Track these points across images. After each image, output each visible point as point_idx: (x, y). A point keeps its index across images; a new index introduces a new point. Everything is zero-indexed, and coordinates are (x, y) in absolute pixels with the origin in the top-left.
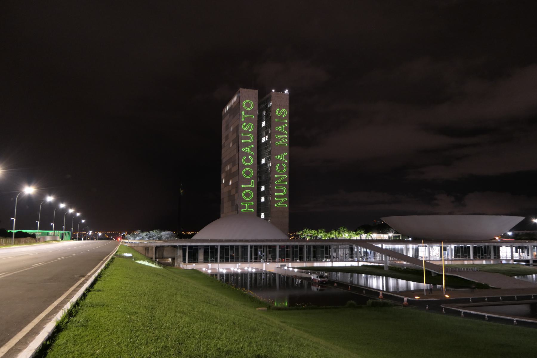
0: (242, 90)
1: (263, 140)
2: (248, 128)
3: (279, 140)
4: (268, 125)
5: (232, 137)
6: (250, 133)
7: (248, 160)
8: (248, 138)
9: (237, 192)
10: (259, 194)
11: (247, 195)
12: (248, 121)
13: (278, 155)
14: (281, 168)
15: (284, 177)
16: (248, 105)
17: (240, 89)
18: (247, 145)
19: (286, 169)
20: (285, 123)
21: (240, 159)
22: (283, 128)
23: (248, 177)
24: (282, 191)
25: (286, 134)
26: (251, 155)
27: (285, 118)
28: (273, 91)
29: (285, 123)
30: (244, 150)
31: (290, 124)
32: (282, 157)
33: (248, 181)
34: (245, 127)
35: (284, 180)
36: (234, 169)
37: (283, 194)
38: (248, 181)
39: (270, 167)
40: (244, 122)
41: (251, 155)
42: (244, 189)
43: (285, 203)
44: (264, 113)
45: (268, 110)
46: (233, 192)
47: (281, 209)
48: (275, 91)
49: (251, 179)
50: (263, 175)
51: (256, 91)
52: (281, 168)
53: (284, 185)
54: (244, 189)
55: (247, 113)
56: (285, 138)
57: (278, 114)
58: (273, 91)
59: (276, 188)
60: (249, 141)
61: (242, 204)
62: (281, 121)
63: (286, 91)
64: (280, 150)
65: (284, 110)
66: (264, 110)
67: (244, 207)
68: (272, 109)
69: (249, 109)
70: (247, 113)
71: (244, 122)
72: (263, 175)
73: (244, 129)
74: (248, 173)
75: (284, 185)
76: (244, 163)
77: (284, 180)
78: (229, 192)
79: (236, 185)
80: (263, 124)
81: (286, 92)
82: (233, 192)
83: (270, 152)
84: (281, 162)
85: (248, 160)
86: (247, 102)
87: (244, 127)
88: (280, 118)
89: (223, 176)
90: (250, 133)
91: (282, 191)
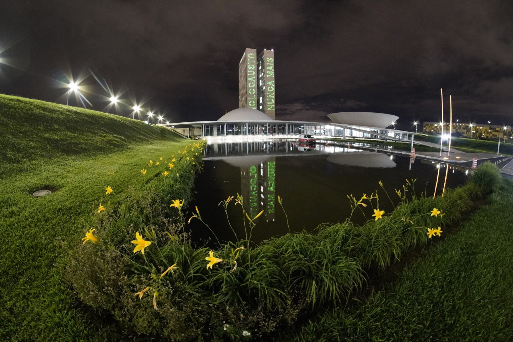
0: (248, 50)
1: (260, 76)
5: (243, 75)
7: (252, 85)
9: (246, 103)
10: (259, 104)
11: (252, 104)
18: (251, 77)
19: (273, 90)
20: (271, 65)
24: (271, 101)
33: (252, 96)
36: (245, 91)
38: (252, 96)
42: (250, 100)
43: (273, 108)
44: (260, 62)
45: (262, 60)
46: (244, 103)
50: (260, 92)
51: (255, 50)
52: (271, 89)
53: (273, 98)
54: (250, 100)
55: (251, 60)
57: (268, 61)
63: (272, 50)
64: (270, 79)
70: (251, 60)
72: (260, 92)
75: (273, 98)
76: (250, 86)
78: (243, 104)
79: (246, 100)
80: (260, 68)
82: (244, 103)
84: (270, 86)
87: (249, 67)
88: (269, 62)
89: (240, 97)
91: (271, 101)
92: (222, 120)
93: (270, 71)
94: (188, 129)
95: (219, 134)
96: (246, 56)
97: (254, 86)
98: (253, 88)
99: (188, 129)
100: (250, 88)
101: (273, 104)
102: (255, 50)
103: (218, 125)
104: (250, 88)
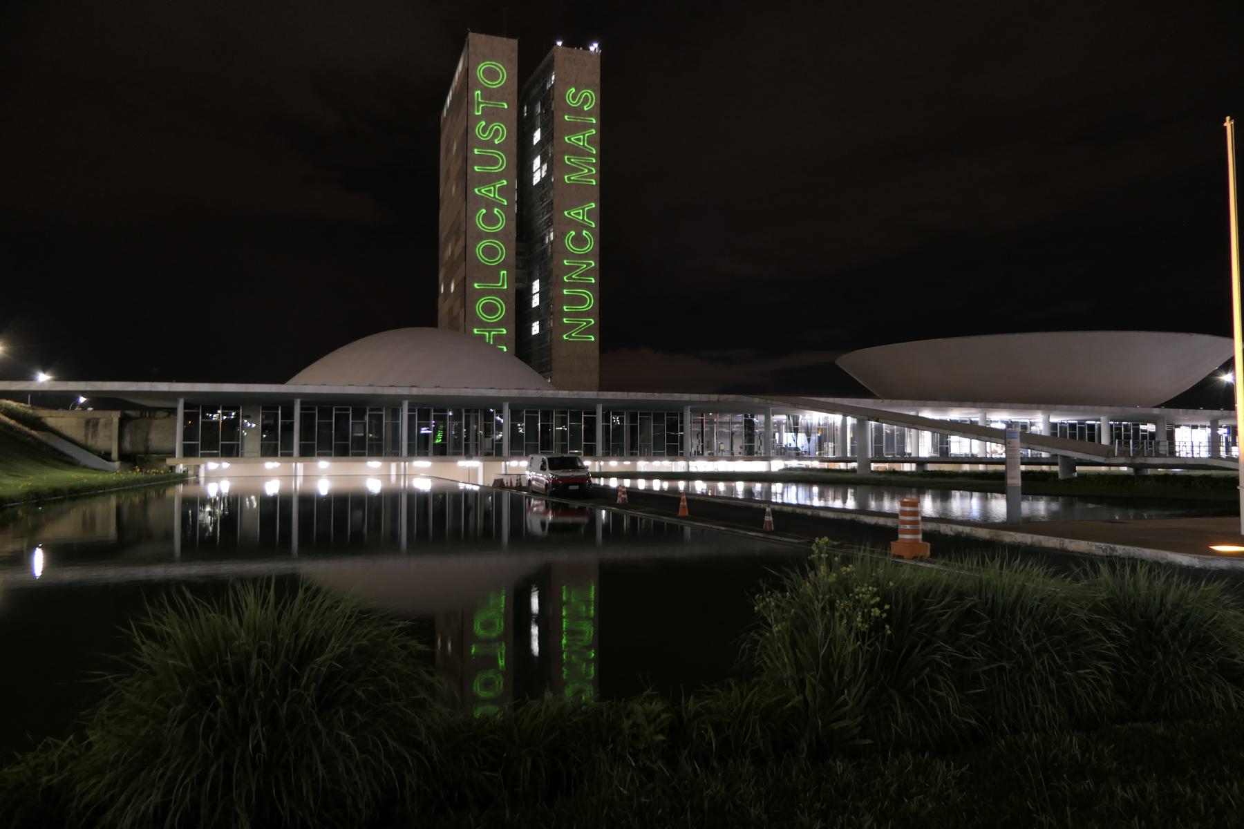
0: (476, 40)
2: (491, 134)
3: (574, 170)
4: (547, 138)
6: (498, 147)
7: (490, 219)
8: (493, 161)
9: (464, 306)
11: (490, 309)
12: (490, 115)
13: (570, 207)
14: (579, 241)
15: (589, 264)
17: (471, 35)
18: (487, 179)
19: (590, 246)
20: (588, 126)
21: (468, 218)
22: (584, 139)
23: (493, 262)
24: (582, 301)
25: (591, 155)
26: (500, 206)
27: (589, 113)
29: (590, 126)
31: (604, 127)
32: (583, 214)
34: (484, 130)
39: (551, 243)
40: (479, 118)
41: (500, 206)
43: (588, 331)
51: (514, 43)
52: (579, 241)
53: (588, 286)
55: (488, 94)
56: (592, 165)
57: (572, 103)
58: (560, 44)
59: (565, 292)
60: (495, 169)
62: (580, 119)
64: (578, 194)
65: (587, 92)
66: (532, 98)
68: (556, 92)
69: (495, 85)
70: (488, 94)
75: (588, 286)
76: (481, 225)
79: (463, 286)
83: (552, 203)
84: (579, 226)
85: (490, 219)
86: (489, 70)
88: (578, 111)
90: (498, 147)
92: (315, 381)
93: (576, 151)
94: (115, 416)
95: (269, 451)
96: (467, 71)
97: (500, 226)
98: (495, 236)
99: (115, 416)
100: (483, 236)
101: (587, 314)
103: (269, 405)
104: (483, 236)
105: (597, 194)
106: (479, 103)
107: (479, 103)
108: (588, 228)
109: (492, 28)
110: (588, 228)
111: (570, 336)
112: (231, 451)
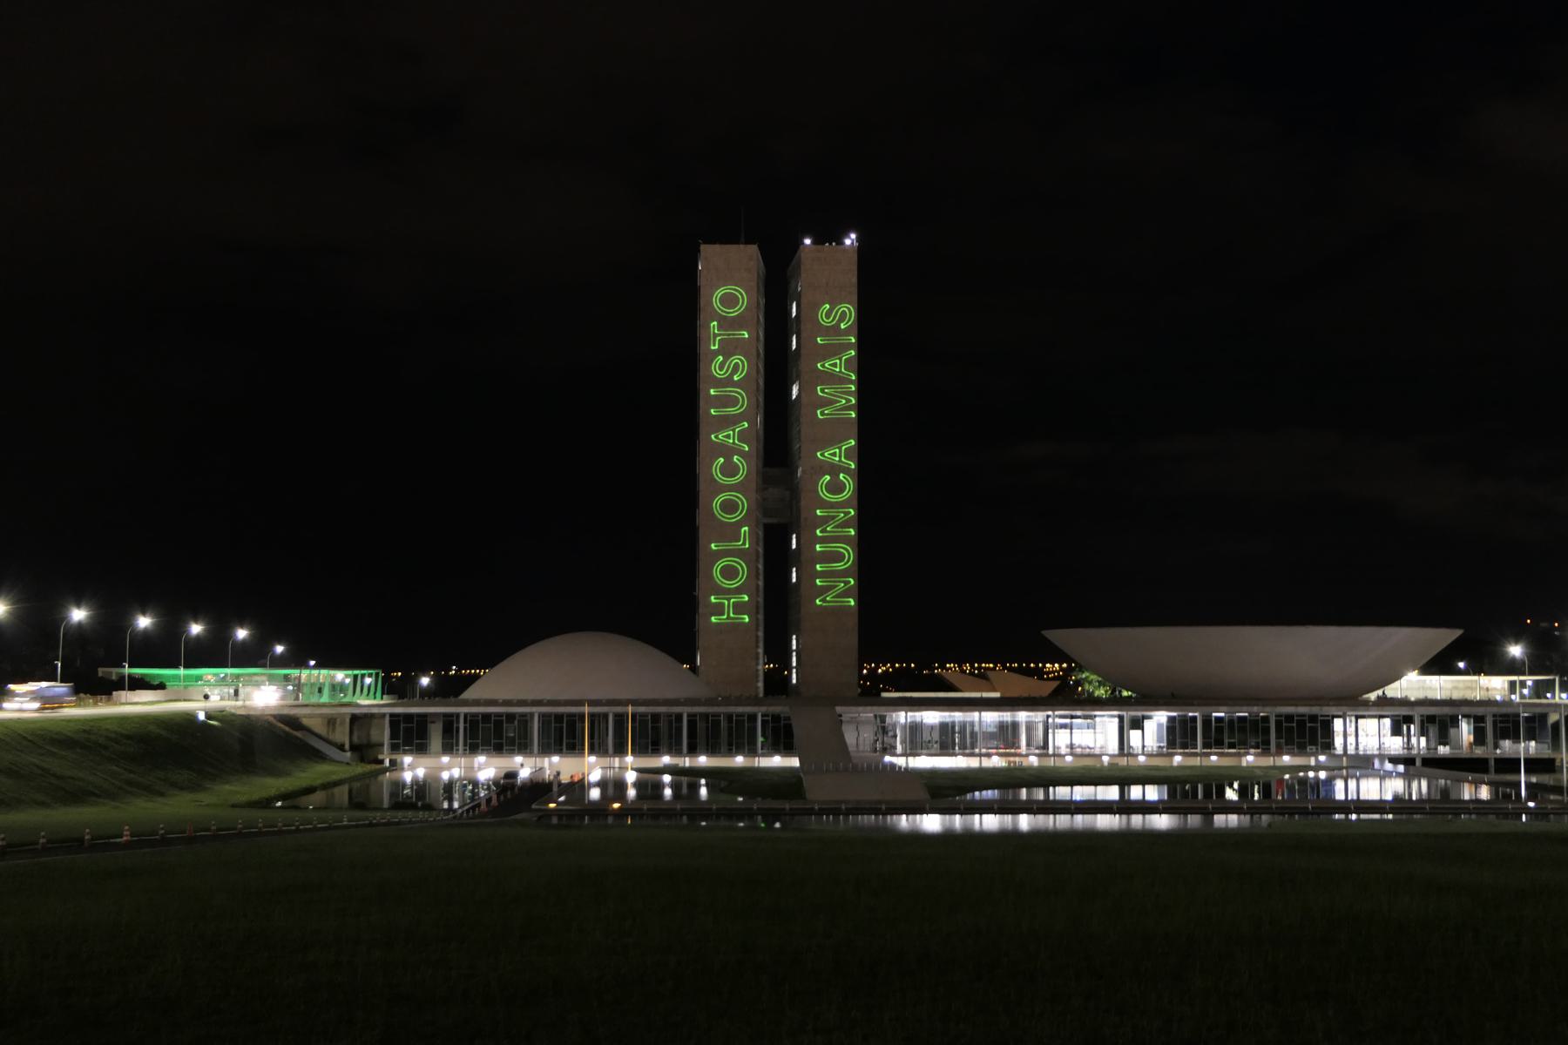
7: (729, 470)
8: (732, 402)
11: (729, 573)
12: (728, 349)
14: (836, 487)
16: (729, 301)
18: (727, 422)
24: (838, 557)
28: (808, 241)
30: (719, 437)
31: (861, 347)
33: (732, 532)
35: (845, 524)
37: (840, 566)
40: (716, 353)
43: (845, 594)
47: (838, 612)
48: (814, 243)
49: (739, 525)
51: (753, 250)
52: (836, 487)
53: (845, 540)
55: (726, 324)
58: (808, 241)
61: (713, 599)
67: (719, 609)
69: (733, 313)
70: (726, 324)
71: (716, 353)
73: (719, 374)
74: (729, 507)
77: (845, 524)
81: (848, 242)
91: (838, 557)
93: (831, 378)
102: (747, 256)
105: (855, 430)
106: (715, 336)
107: (715, 336)
108: (847, 471)
109: (727, 237)
110: (847, 471)
111: (824, 600)
112: (421, 749)
